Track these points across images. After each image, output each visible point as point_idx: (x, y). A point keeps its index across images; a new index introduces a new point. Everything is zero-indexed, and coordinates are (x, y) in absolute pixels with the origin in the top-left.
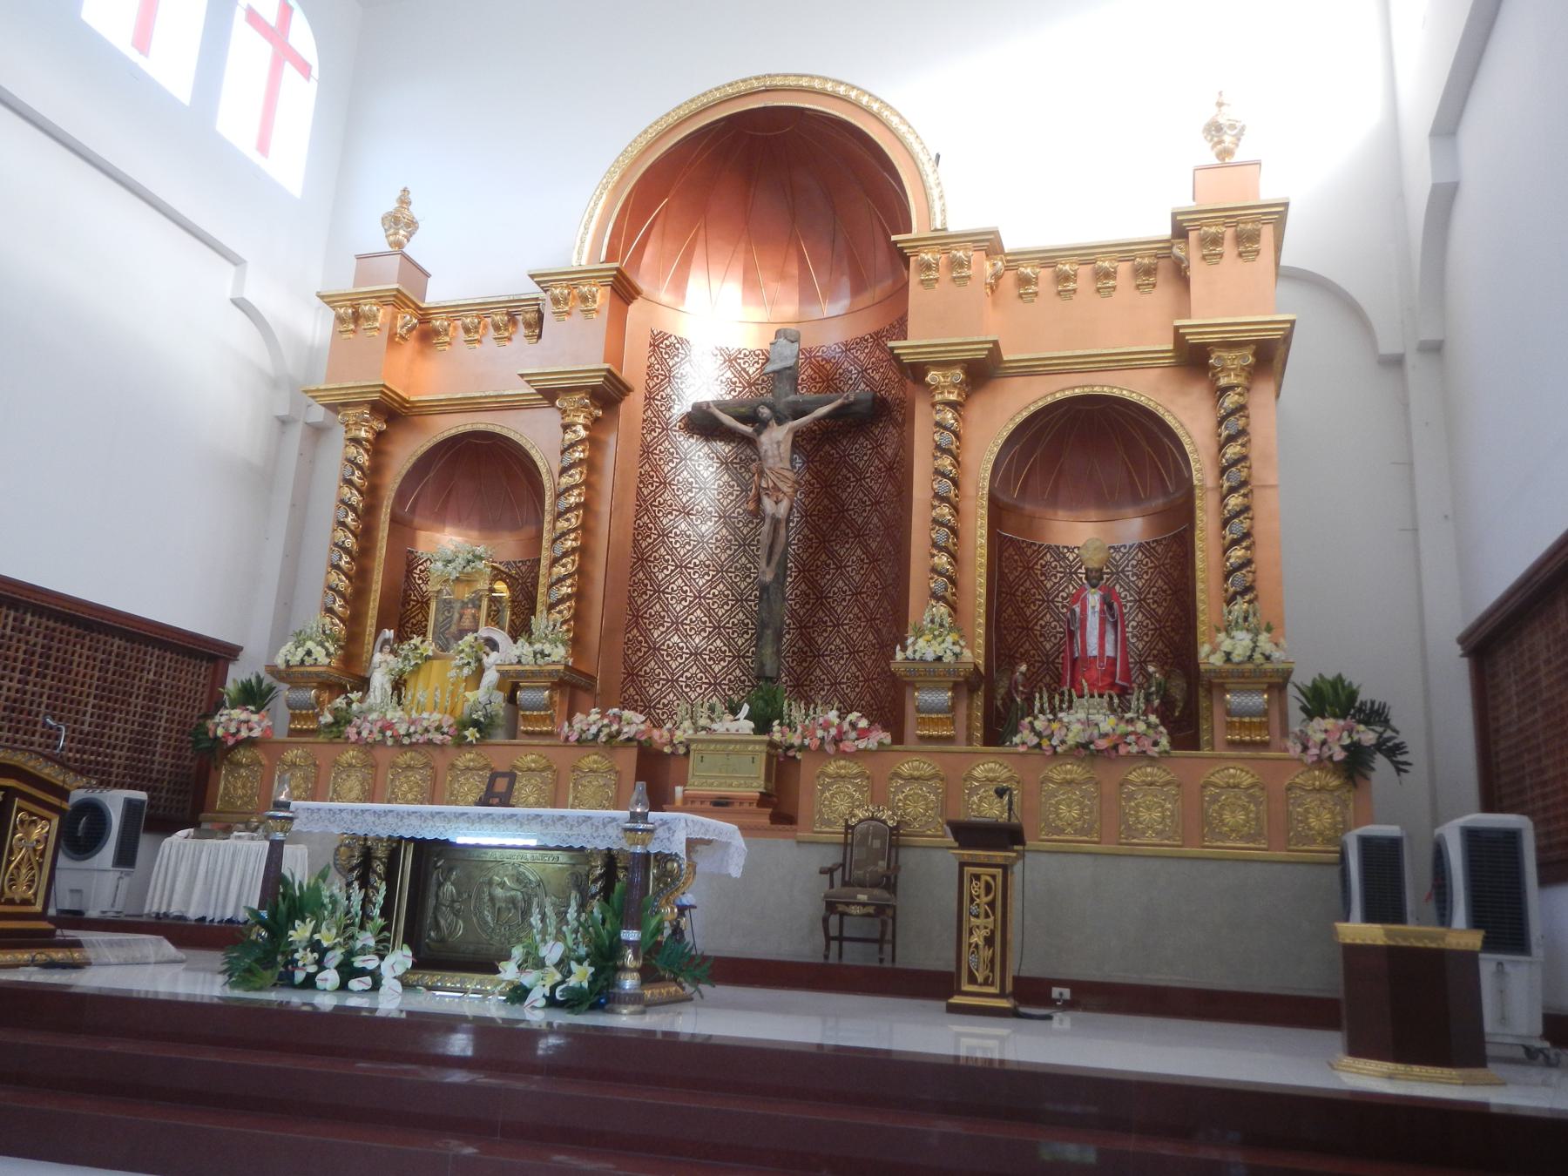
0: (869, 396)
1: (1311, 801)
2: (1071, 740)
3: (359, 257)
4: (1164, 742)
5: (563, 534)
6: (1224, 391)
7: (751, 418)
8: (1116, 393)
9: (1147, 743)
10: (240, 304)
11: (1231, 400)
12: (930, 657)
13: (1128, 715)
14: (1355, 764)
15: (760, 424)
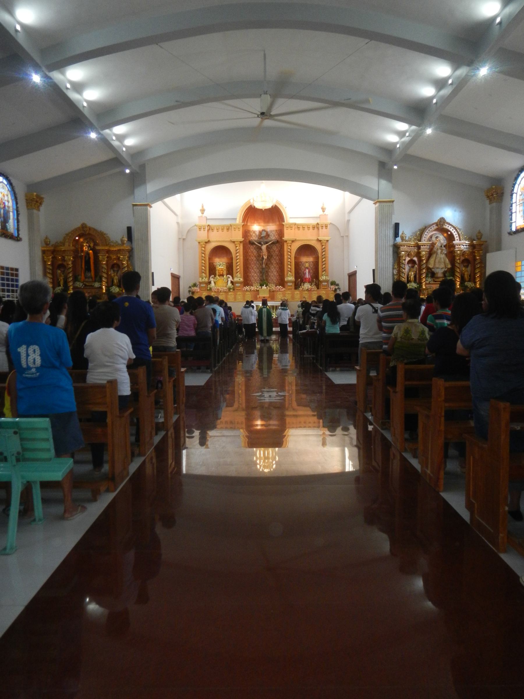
0: (276, 240)
1: (331, 294)
2: (306, 289)
3: (199, 217)
4: (316, 289)
5: (238, 262)
6: (323, 245)
7: (260, 243)
8: (310, 244)
9: (314, 289)
10: (178, 223)
11: (324, 247)
12: (290, 280)
13: (312, 286)
14: (336, 290)
15: (262, 245)
